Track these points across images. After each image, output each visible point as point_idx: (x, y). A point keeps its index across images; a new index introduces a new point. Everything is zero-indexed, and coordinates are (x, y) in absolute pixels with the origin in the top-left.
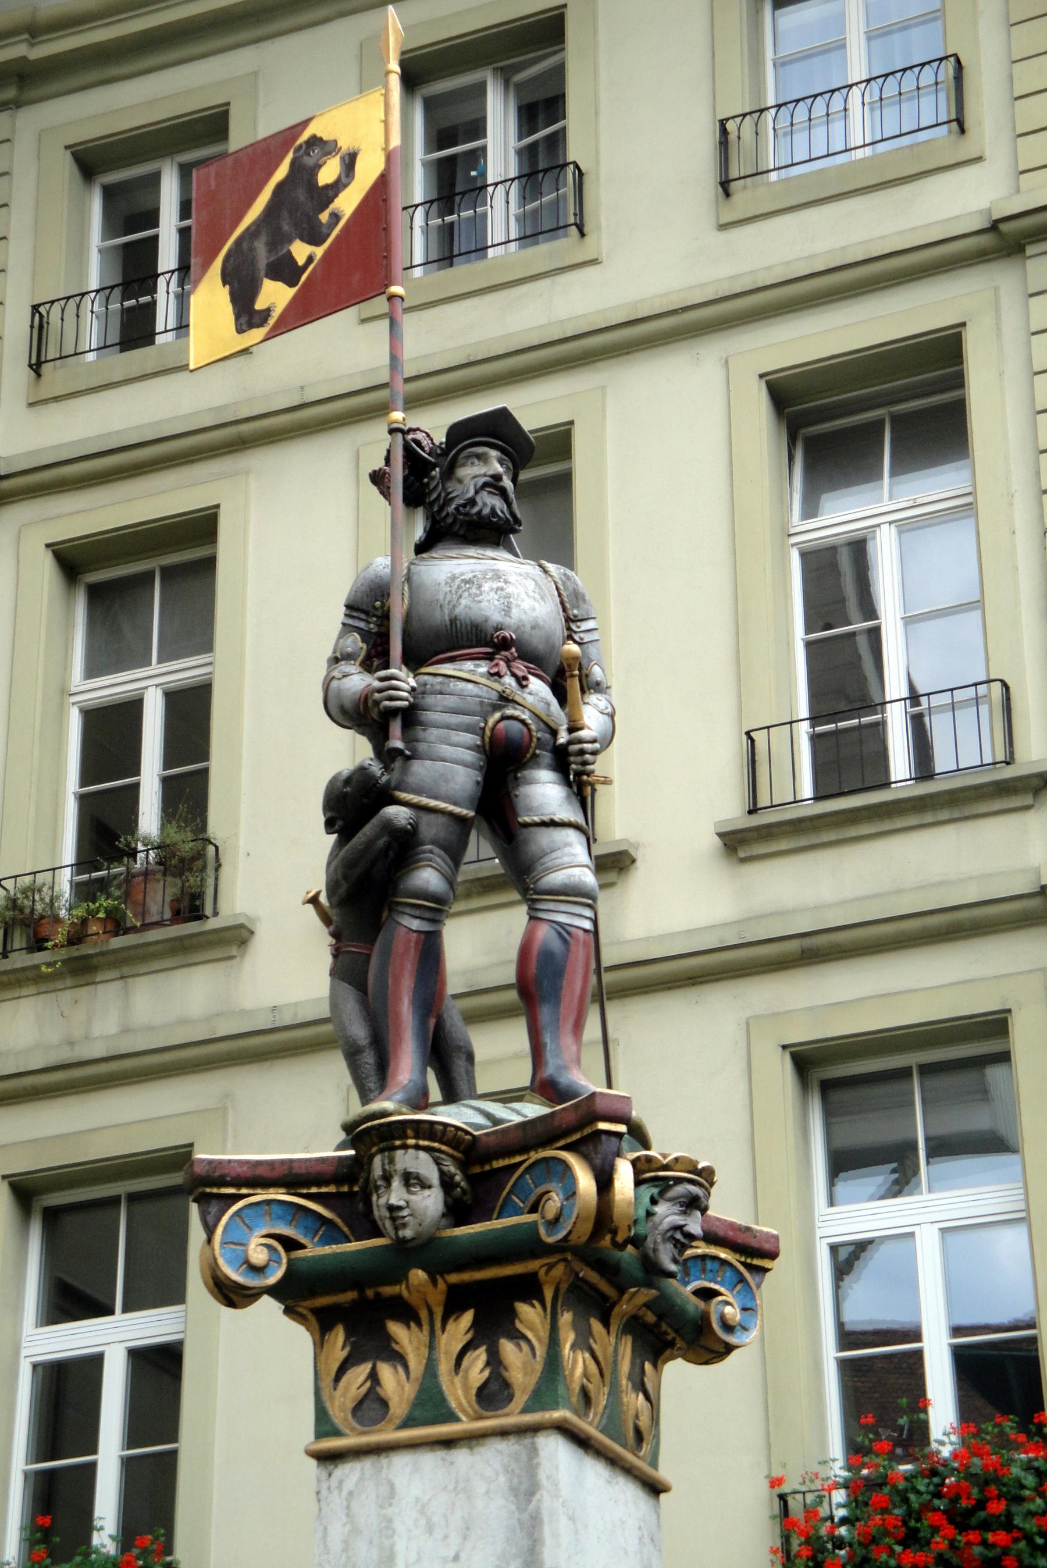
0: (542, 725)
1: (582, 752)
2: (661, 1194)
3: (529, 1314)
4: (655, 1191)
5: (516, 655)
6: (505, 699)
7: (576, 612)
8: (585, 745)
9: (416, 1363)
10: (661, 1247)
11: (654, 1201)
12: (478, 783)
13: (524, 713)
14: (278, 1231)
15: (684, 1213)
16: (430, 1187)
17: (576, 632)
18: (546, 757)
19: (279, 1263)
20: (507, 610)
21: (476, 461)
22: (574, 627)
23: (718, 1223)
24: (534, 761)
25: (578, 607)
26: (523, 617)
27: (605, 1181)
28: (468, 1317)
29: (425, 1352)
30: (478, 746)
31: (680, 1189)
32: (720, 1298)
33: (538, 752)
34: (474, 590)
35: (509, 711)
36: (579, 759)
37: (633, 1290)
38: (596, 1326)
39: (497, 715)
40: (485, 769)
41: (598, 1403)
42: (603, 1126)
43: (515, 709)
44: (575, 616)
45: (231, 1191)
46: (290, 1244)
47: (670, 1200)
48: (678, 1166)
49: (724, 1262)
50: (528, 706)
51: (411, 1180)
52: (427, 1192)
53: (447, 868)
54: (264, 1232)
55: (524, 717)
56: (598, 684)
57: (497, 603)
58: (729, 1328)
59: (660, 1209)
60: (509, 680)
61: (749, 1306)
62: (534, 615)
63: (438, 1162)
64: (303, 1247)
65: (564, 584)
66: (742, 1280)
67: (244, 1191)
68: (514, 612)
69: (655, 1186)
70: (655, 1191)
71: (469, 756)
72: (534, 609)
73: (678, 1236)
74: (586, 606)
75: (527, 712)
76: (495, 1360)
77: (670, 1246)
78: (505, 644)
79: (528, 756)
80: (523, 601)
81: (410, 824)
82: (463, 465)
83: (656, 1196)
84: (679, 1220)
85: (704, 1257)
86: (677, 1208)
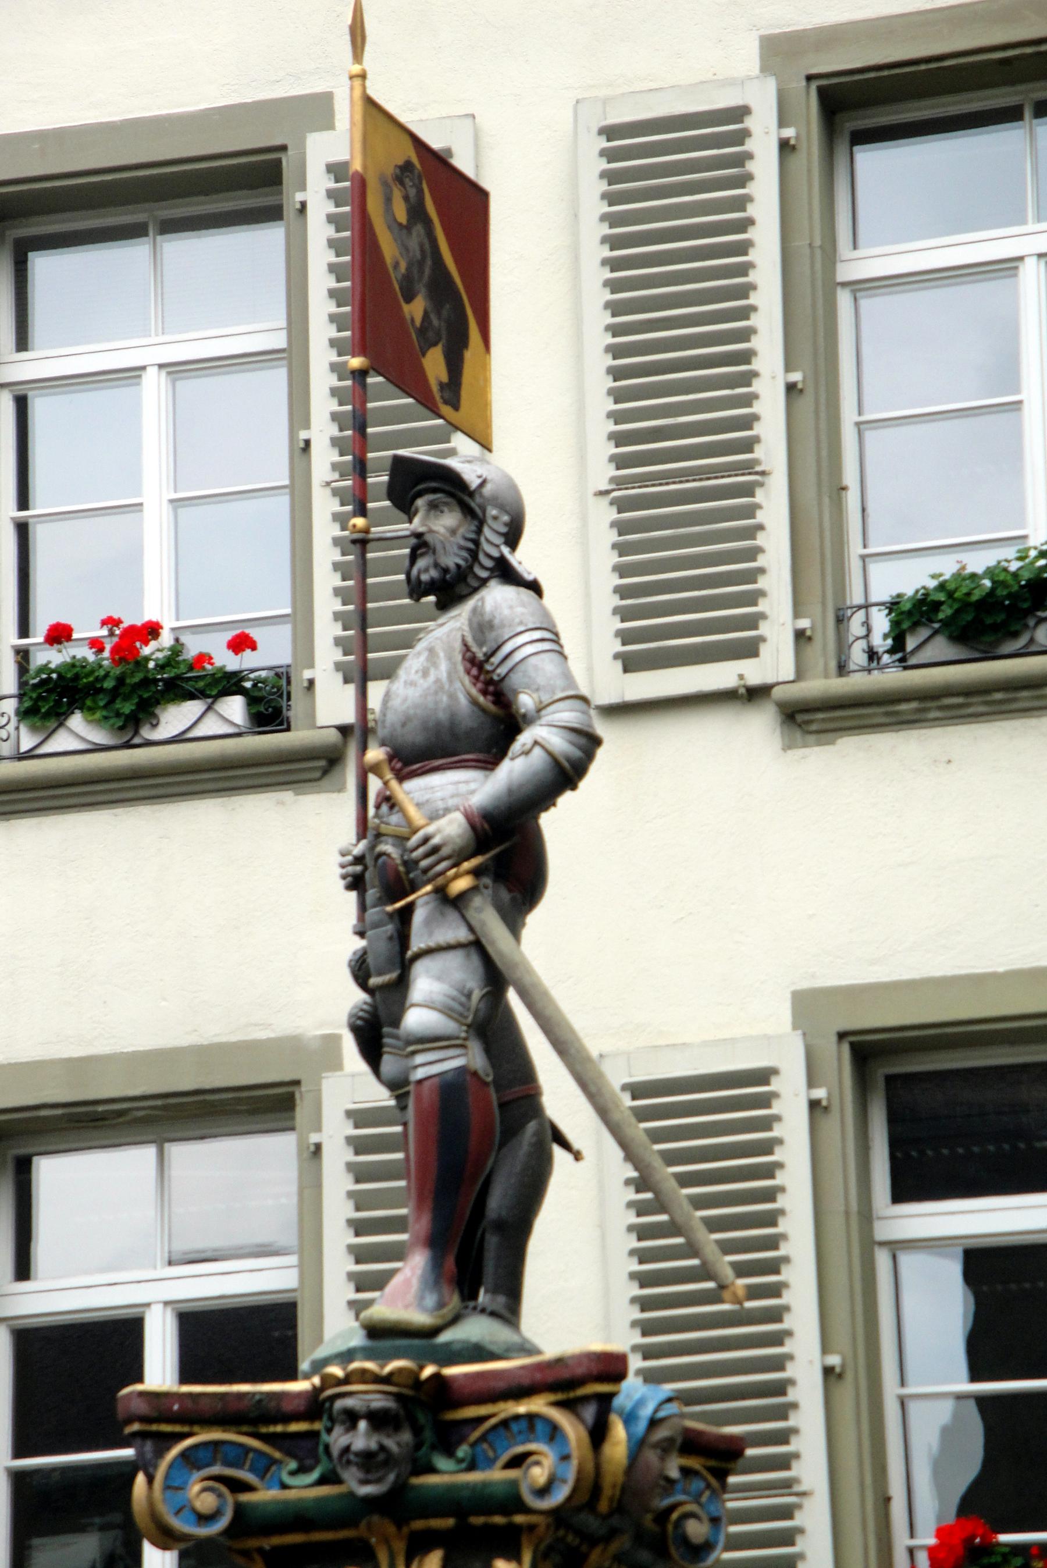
7: (484, 649)
22: (488, 667)
49: (531, 1418)
74: (493, 634)
75: (390, 840)
85: (505, 1423)
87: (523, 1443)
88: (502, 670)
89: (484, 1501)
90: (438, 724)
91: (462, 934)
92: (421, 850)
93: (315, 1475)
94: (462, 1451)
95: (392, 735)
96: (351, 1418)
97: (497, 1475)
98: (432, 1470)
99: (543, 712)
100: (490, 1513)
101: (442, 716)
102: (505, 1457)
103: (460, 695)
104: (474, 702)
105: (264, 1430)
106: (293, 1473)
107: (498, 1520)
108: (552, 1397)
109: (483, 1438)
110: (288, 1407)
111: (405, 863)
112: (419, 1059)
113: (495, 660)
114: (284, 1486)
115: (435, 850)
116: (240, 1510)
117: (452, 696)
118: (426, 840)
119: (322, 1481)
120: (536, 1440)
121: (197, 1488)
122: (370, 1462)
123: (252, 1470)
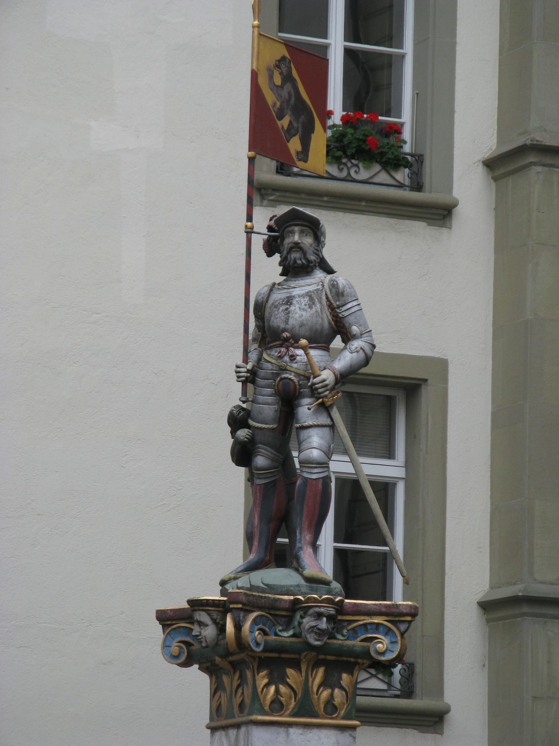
0: (302, 377)
1: (317, 389)
2: (305, 613)
3: (249, 674)
4: (302, 613)
5: (293, 342)
6: (283, 369)
7: (338, 303)
8: (317, 386)
9: (228, 691)
10: (308, 636)
11: (302, 617)
12: (276, 411)
13: (290, 374)
14: (183, 639)
15: (315, 620)
16: (207, 625)
17: (340, 313)
18: (306, 391)
19: (184, 653)
20: (287, 322)
21: (291, 235)
22: (338, 311)
23: (375, 607)
24: (301, 396)
25: (339, 300)
26: (294, 322)
27: (238, 627)
28: (237, 674)
29: (230, 687)
30: (274, 394)
31: (311, 611)
32: (376, 641)
33: (301, 390)
34: (276, 312)
35: (283, 376)
36: (316, 392)
37: (305, 653)
38: (290, 672)
39: (279, 379)
40: (280, 403)
41: (289, 704)
42: (232, 606)
43: (287, 373)
44: (337, 305)
45: (169, 623)
46: (188, 644)
47: (309, 615)
48: (310, 601)
49: (378, 624)
50: (293, 370)
51: (201, 624)
52: (207, 628)
53: (269, 453)
54: (180, 639)
55: (290, 377)
56: (355, 335)
57: (283, 318)
58: (383, 654)
59: (305, 620)
60: (287, 358)
61: (394, 640)
62: (301, 319)
63: (209, 615)
64: (192, 645)
65: (331, 290)
66: (390, 630)
67: (174, 622)
68: (291, 322)
69: (302, 611)
70: (302, 613)
71: (270, 399)
72: (302, 316)
73: (315, 630)
75: (293, 374)
76: (243, 693)
77: (313, 635)
78: (286, 340)
79: (297, 394)
80: (296, 313)
81: (246, 438)
82: (286, 237)
83: (303, 615)
84: (313, 624)
85: (365, 625)
86: (313, 619)
87: (372, 633)
88: (346, 314)
89: (351, 652)
90: (317, 330)
91: (328, 422)
92: (320, 385)
93: (291, 633)
94: (345, 632)
95: (292, 329)
96: (319, 616)
97: (356, 643)
98: (335, 638)
99: (363, 336)
100: (351, 657)
101: (319, 327)
102: (363, 637)
103: (326, 319)
104: (330, 323)
105: (272, 612)
106: (280, 631)
107: (352, 660)
108: (387, 618)
109: (353, 629)
110: (283, 605)
111: (300, 385)
112: (316, 470)
113: (344, 308)
114: (276, 635)
115: (327, 385)
116: (266, 642)
117: (322, 319)
118: (324, 381)
119: (293, 636)
120: (379, 633)
121: (257, 633)
122: (320, 633)
123: (268, 628)
